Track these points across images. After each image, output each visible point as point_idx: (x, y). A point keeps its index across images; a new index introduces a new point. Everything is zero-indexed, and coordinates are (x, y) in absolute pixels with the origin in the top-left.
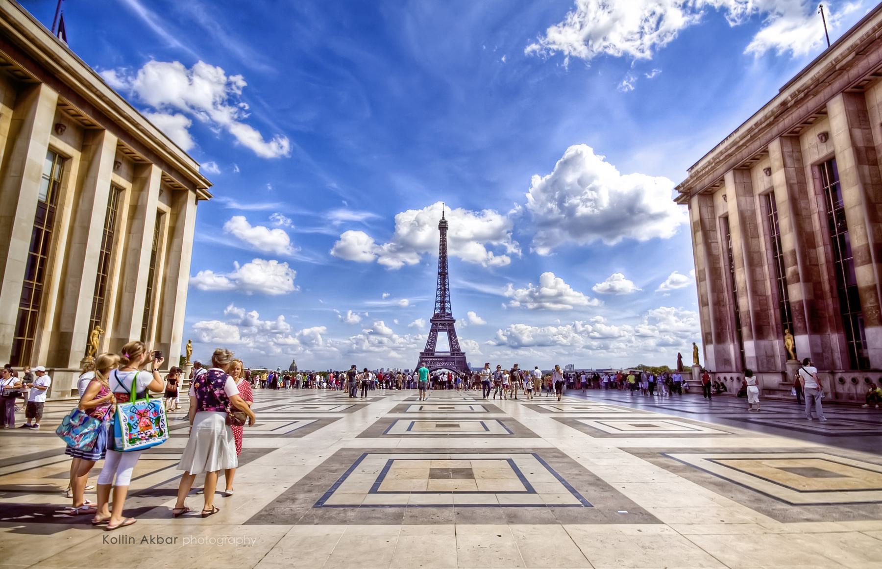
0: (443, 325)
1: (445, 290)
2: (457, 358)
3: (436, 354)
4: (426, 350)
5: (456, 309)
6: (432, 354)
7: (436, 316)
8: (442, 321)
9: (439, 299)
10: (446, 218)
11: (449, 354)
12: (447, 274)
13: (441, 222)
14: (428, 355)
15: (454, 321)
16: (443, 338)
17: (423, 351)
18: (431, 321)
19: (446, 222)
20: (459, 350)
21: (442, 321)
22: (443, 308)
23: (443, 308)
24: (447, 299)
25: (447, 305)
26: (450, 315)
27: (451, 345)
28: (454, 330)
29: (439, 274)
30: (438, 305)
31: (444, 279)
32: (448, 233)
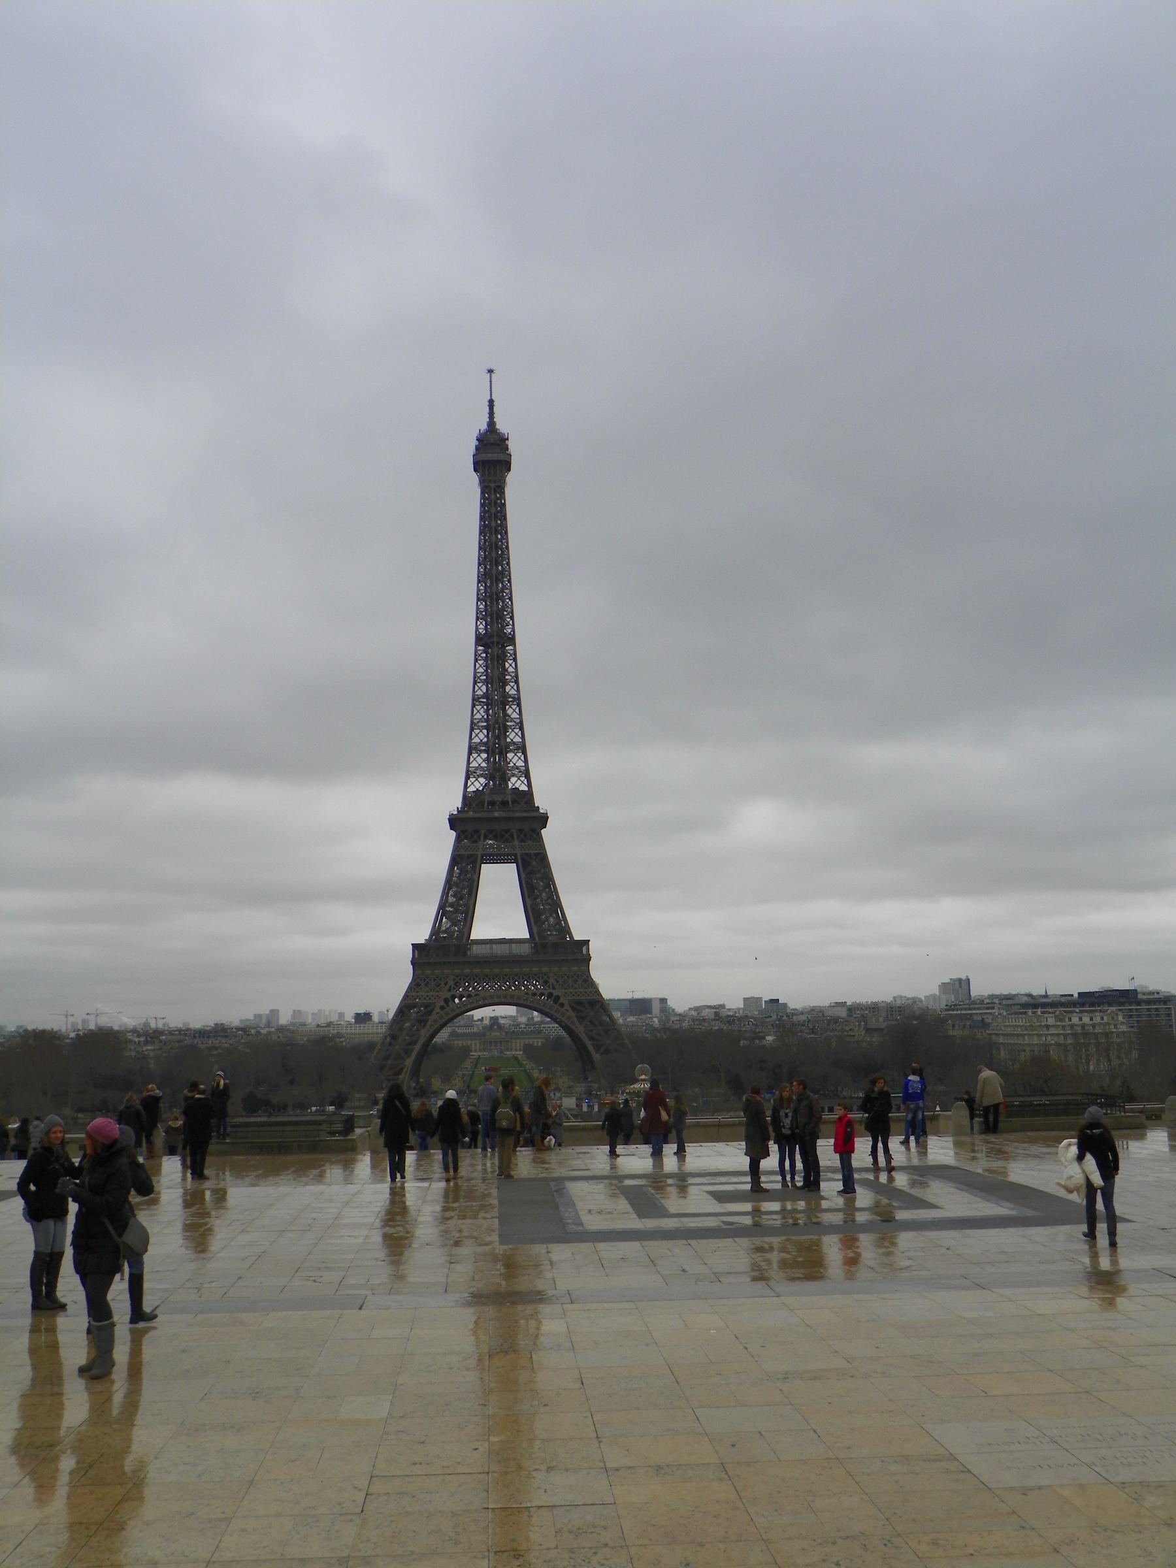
1: (504, 701)
2: (554, 952)
3: (476, 950)
4: (435, 932)
5: (553, 776)
7: (469, 800)
8: (498, 823)
9: (481, 736)
10: (502, 426)
11: (526, 949)
12: (512, 640)
14: (447, 959)
15: (543, 820)
18: (454, 822)
20: (566, 930)
21: (498, 823)
22: (498, 773)
23: (498, 773)
24: (513, 736)
25: (515, 759)
26: (528, 796)
27: (533, 915)
28: (543, 858)
29: (479, 640)
30: (479, 760)
32: (512, 480)
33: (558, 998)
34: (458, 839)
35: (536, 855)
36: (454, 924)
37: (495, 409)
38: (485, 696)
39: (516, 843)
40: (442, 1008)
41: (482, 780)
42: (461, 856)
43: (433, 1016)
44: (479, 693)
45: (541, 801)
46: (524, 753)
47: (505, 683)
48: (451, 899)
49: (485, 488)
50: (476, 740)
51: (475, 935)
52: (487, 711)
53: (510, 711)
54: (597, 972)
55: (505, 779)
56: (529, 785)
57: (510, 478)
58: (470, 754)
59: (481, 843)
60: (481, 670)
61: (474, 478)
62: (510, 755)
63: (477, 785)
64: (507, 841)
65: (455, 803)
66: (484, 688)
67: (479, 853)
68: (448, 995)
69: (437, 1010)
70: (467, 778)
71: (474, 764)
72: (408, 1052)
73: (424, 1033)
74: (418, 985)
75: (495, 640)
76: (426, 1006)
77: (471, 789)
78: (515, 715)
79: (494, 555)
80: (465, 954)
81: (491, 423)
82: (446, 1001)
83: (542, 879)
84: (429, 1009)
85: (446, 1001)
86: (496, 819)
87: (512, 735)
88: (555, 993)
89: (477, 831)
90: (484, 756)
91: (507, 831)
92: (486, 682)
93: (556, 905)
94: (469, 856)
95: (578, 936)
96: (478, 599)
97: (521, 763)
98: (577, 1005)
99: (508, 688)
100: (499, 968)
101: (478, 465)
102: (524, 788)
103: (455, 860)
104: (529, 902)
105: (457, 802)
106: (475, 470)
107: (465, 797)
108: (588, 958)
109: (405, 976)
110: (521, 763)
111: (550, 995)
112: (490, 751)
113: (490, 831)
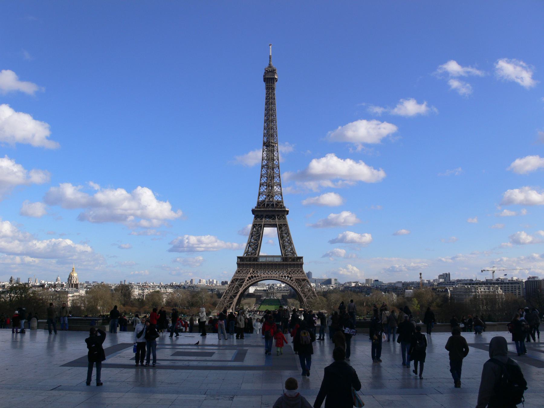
0: (269, 217)
2: (290, 262)
3: (261, 260)
4: (247, 252)
6: (256, 259)
7: (260, 204)
8: (270, 212)
9: (264, 180)
11: (279, 260)
13: (267, 72)
14: (249, 262)
15: (287, 212)
16: (270, 233)
17: (241, 254)
18: (253, 211)
19: (273, 72)
20: (294, 253)
21: (270, 212)
23: (270, 195)
24: (276, 180)
27: (283, 247)
28: (286, 225)
29: (264, 144)
30: (264, 189)
31: (273, 151)
33: (291, 278)
34: (255, 217)
35: (284, 224)
36: (253, 249)
37: (272, 59)
38: (266, 165)
39: (277, 220)
40: (248, 280)
41: (265, 196)
42: (256, 224)
43: (244, 283)
44: (264, 164)
45: (287, 205)
46: (280, 186)
47: (274, 160)
48: (252, 240)
49: (267, 88)
50: (263, 181)
51: (261, 254)
52: (267, 171)
53: (275, 171)
54: (306, 269)
55: (272, 197)
56: (282, 199)
57: (277, 85)
58: (260, 186)
59: (264, 220)
60: (265, 155)
61: (263, 85)
62: (275, 187)
63: (262, 198)
64: (273, 219)
65: (254, 205)
66: (266, 162)
67: (263, 224)
68: (250, 276)
69: (246, 281)
70: (259, 195)
71: (262, 190)
72: (235, 296)
73: (241, 290)
74: (239, 272)
75: (269, 145)
76: (242, 279)
77: (261, 199)
78: (277, 172)
79: (270, 112)
80: (257, 261)
81: (270, 64)
82: (249, 277)
83: (286, 234)
84: (242, 280)
85: (249, 277)
86: (269, 211)
87: (276, 180)
88: (290, 276)
89: (262, 215)
90: (266, 187)
91: (273, 215)
92: (266, 160)
93: (291, 243)
94: (259, 224)
95: (299, 255)
96: (265, 129)
97: (279, 190)
98: (298, 280)
99: (275, 162)
100: (270, 265)
101: (266, 80)
102: (280, 199)
103: (254, 226)
104: (281, 242)
105: (255, 204)
106: (264, 81)
107: (258, 203)
108: (302, 264)
109: (235, 268)
110: (279, 190)
111: (288, 277)
112: (268, 186)
113: (267, 215)
